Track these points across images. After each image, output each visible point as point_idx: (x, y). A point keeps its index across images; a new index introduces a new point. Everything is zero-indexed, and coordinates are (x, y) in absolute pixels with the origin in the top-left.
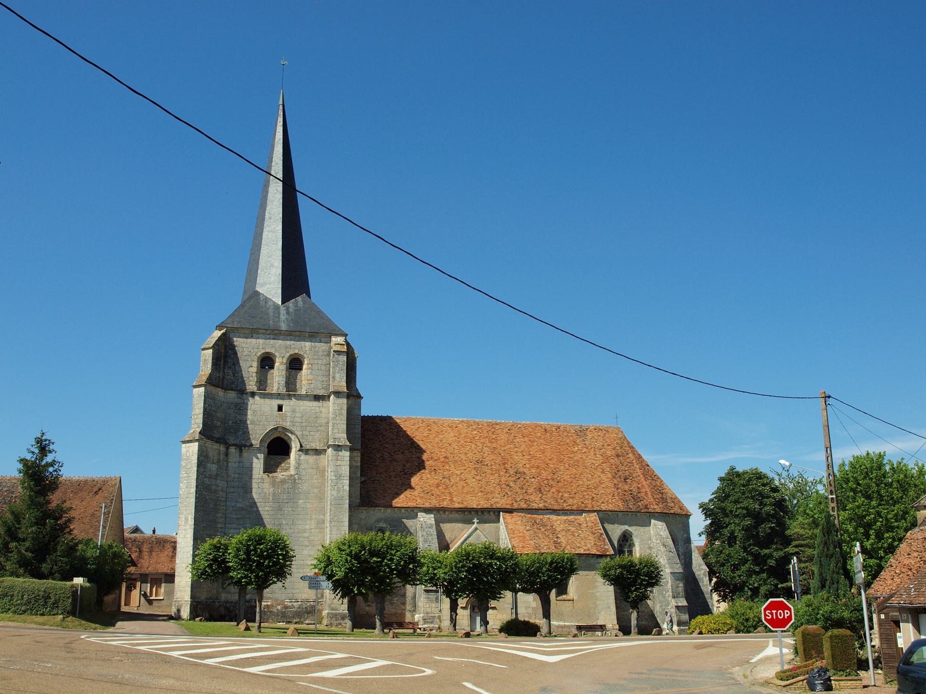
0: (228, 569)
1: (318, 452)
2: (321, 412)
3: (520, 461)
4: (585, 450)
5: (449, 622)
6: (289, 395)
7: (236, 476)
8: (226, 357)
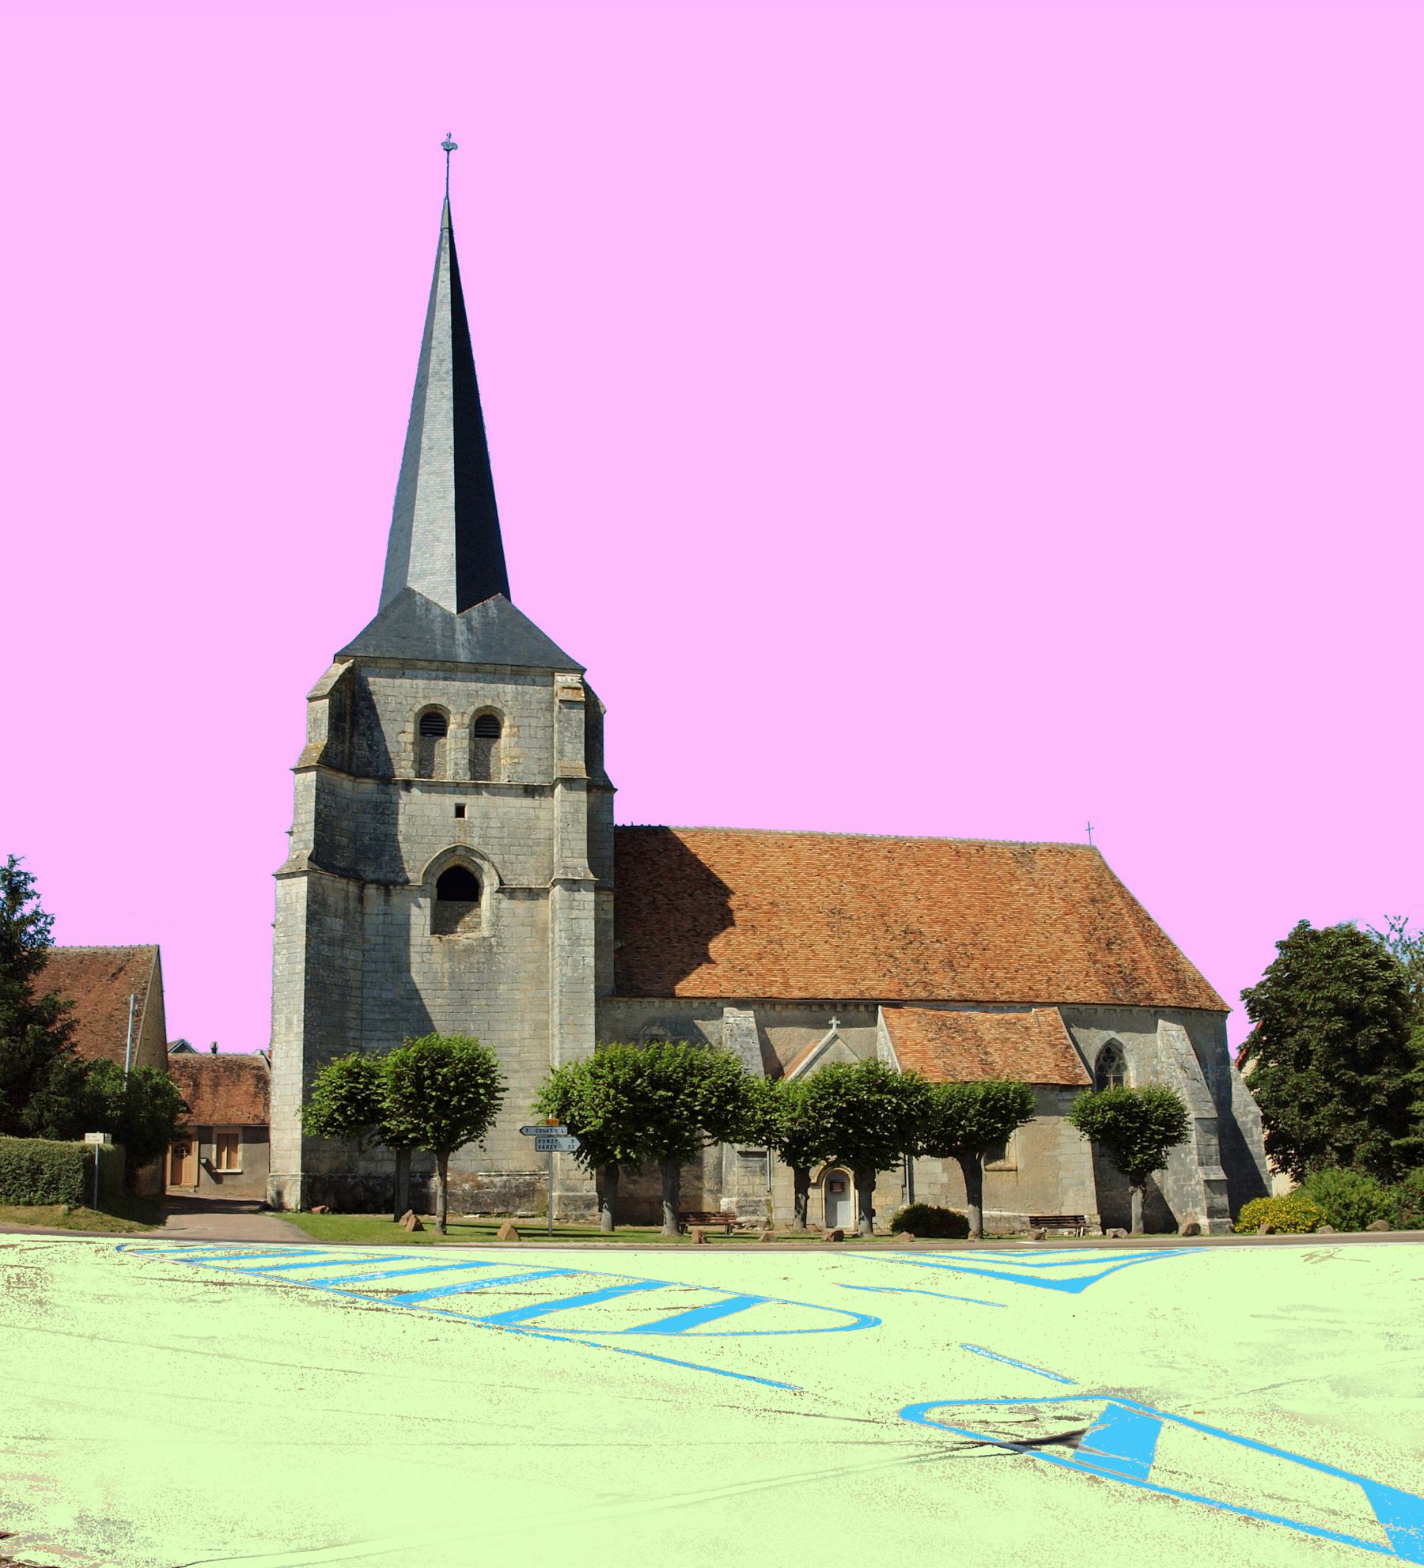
0: (382, 1114)
1: (533, 894)
2: (537, 818)
3: (913, 911)
4: (1032, 889)
5: (793, 1212)
6: (477, 786)
7: (380, 940)
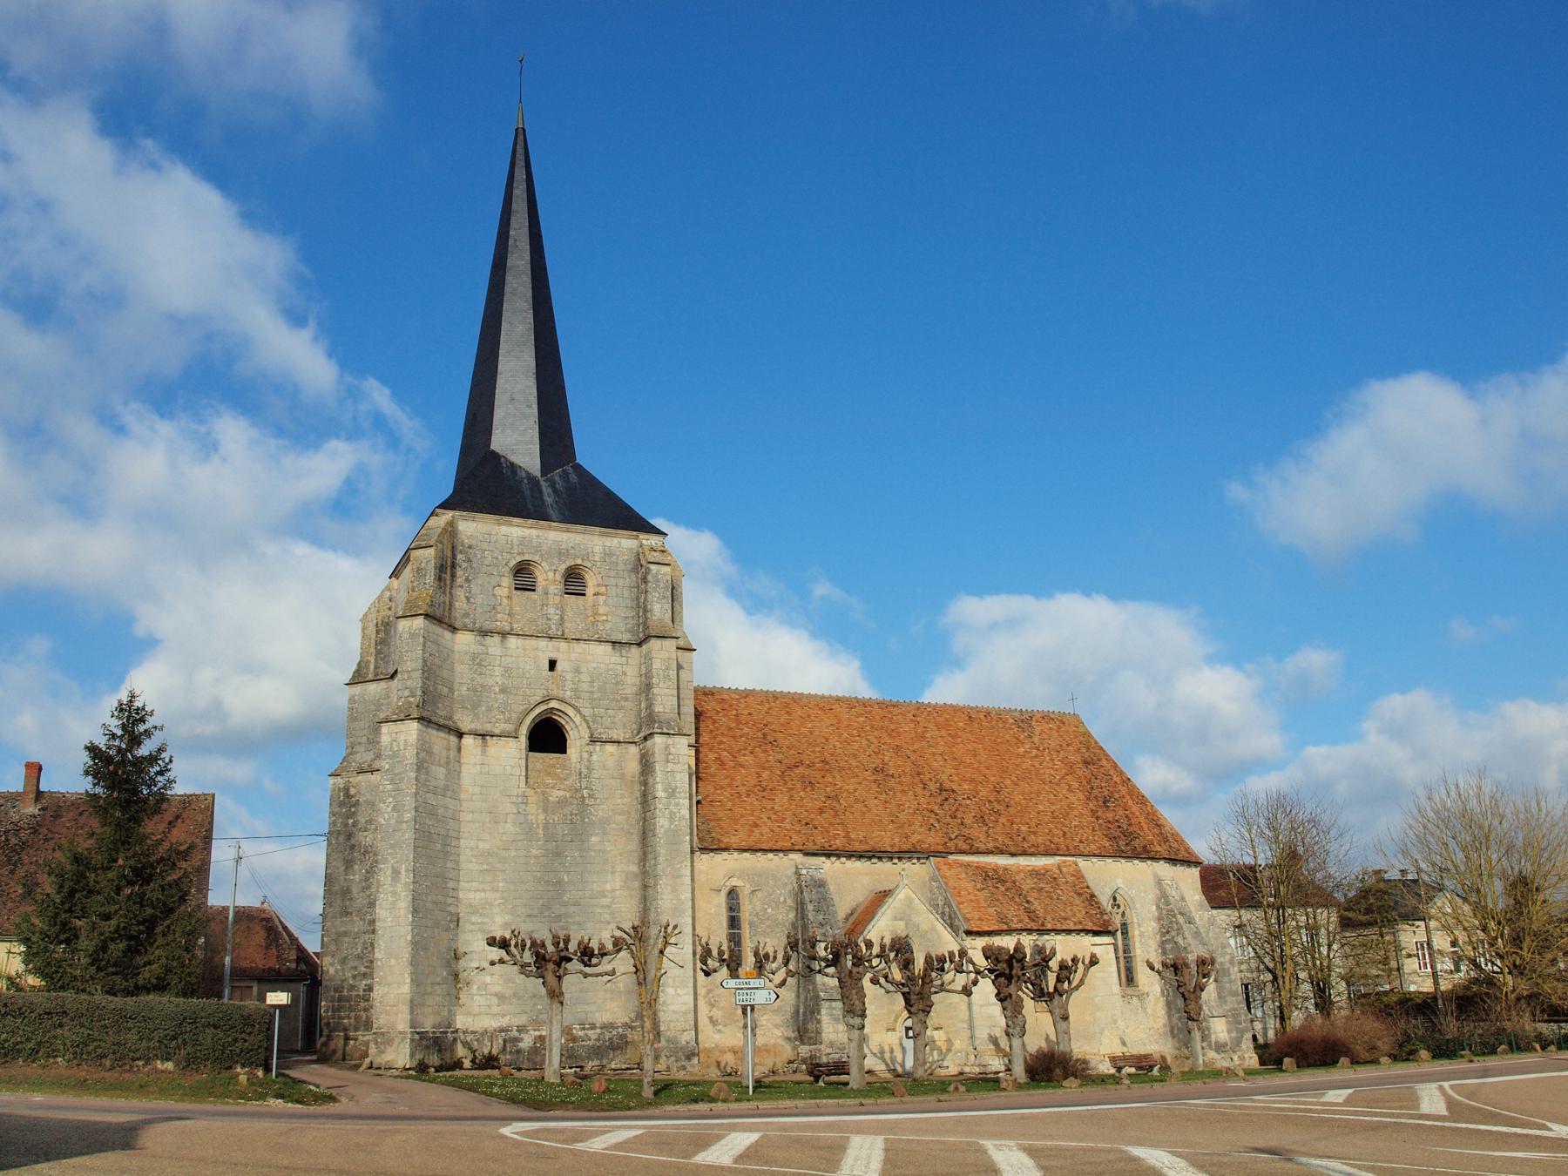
2: (624, 673)
7: (477, 790)
8: (453, 566)
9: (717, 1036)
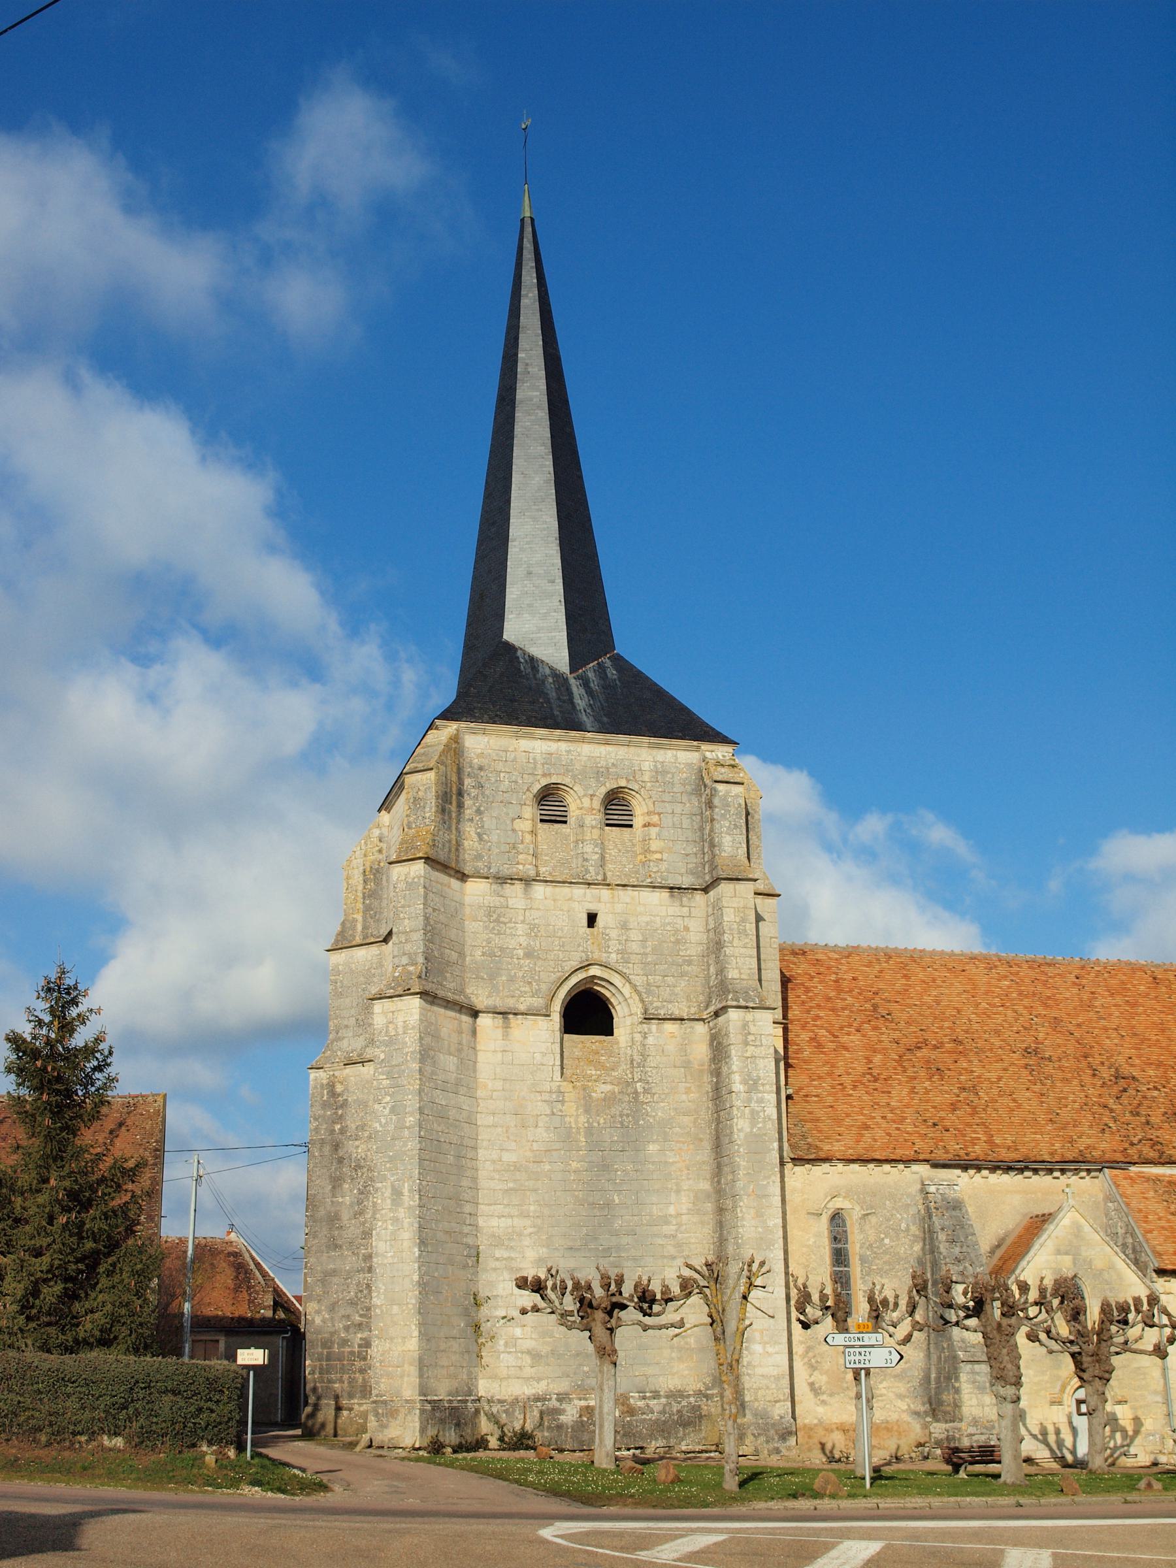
2: (687, 929)
7: (499, 1085)
8: (460, 794)
9: (821, 1410)
